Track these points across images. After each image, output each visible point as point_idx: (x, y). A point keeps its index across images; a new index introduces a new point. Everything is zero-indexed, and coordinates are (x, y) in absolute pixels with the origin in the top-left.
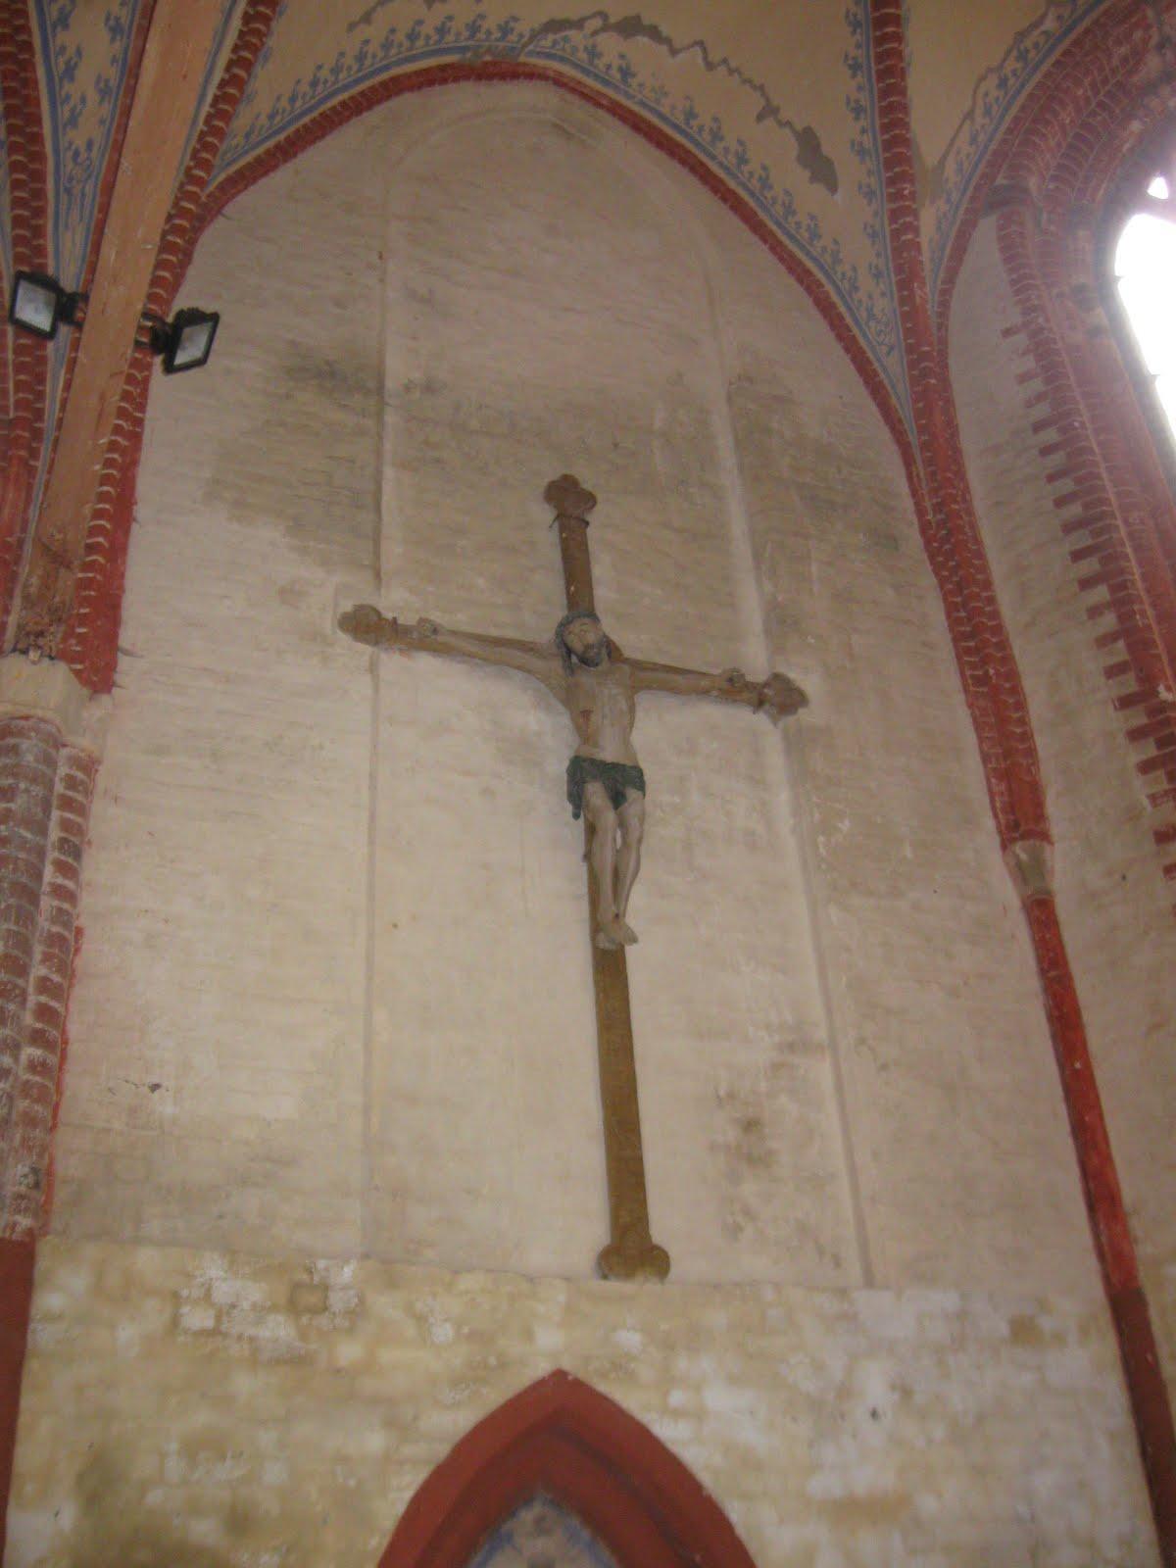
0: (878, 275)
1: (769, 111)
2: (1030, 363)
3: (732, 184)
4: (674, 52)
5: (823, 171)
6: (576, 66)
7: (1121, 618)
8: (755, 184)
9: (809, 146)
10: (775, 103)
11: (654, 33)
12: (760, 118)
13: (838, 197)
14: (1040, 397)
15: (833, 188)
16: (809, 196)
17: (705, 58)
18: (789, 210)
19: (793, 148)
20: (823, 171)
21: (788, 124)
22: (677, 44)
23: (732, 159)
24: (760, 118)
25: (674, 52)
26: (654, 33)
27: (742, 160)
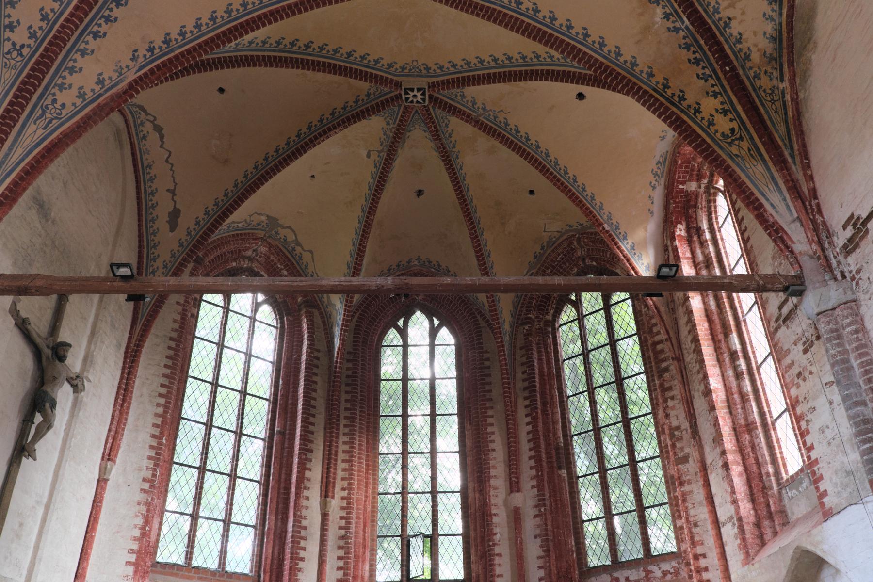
0: (165, 266)
1: (173, 192)
2: (178, 318)
3: (143, 196)
4: (161, 147)
5: (173, 224)
6: (134, 121)
7: (164, 412)
8: (150, 204)
9: (175, 215)
10: (177, 192)
11: (162, 137)
12: (168, 190)
13: (171, 234)
14: (176, 330)
15: (172, 230)
16: (162, 223)
17: (168, 158)
18: (153, 220)
19: (171, 209)
20: (173, 224)
21: (175, 202)
22: (164, 146)
23: (150, 190)
24: (168, 190)
25: (161, 147)
26: (162, 137)
27: (152, 193)
